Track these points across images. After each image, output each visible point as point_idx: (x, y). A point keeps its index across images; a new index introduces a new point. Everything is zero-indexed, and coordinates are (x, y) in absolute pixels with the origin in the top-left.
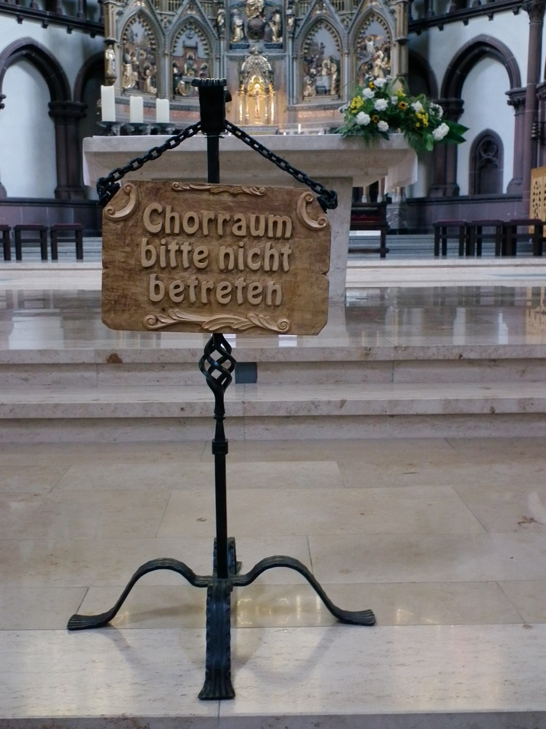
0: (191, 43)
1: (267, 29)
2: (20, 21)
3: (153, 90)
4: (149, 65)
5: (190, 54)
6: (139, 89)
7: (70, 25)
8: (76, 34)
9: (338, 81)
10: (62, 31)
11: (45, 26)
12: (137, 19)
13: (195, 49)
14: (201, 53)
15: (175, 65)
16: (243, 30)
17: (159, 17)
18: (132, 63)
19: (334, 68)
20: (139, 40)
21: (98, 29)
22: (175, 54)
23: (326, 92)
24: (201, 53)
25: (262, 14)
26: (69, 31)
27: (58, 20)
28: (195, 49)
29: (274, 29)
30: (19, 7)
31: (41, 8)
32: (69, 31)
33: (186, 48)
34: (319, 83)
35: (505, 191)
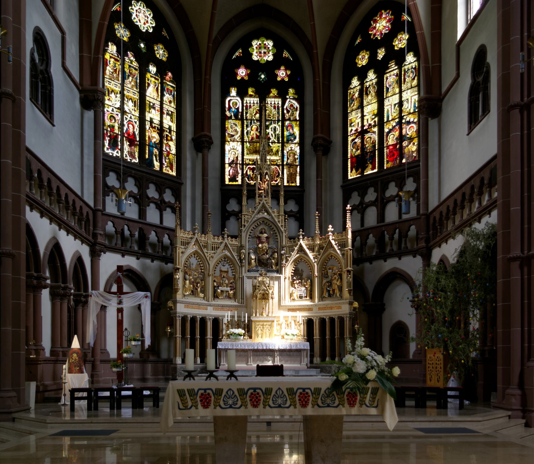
2: (123, 256)
3: (202, 295)
4: (200, 281)
6: (193, 294)
7: (153, 258)
8: (156, 263)
10: (148, 261)
11: (138, 259)
12: (193, 256)
13: (227, 272)
15: (214, 281)
16: (255, 261)
17: (206, 254)
18: (190, 280)
20: (194, 267)
21: (171, 259)
22: (215, 275)
24: (230, 274)
26: (152, 261)
27: (146, 255)
30: (123, 248)
31: (136, 248)
32: (152, 261)
33: (221, 271)
35: (411, 357)
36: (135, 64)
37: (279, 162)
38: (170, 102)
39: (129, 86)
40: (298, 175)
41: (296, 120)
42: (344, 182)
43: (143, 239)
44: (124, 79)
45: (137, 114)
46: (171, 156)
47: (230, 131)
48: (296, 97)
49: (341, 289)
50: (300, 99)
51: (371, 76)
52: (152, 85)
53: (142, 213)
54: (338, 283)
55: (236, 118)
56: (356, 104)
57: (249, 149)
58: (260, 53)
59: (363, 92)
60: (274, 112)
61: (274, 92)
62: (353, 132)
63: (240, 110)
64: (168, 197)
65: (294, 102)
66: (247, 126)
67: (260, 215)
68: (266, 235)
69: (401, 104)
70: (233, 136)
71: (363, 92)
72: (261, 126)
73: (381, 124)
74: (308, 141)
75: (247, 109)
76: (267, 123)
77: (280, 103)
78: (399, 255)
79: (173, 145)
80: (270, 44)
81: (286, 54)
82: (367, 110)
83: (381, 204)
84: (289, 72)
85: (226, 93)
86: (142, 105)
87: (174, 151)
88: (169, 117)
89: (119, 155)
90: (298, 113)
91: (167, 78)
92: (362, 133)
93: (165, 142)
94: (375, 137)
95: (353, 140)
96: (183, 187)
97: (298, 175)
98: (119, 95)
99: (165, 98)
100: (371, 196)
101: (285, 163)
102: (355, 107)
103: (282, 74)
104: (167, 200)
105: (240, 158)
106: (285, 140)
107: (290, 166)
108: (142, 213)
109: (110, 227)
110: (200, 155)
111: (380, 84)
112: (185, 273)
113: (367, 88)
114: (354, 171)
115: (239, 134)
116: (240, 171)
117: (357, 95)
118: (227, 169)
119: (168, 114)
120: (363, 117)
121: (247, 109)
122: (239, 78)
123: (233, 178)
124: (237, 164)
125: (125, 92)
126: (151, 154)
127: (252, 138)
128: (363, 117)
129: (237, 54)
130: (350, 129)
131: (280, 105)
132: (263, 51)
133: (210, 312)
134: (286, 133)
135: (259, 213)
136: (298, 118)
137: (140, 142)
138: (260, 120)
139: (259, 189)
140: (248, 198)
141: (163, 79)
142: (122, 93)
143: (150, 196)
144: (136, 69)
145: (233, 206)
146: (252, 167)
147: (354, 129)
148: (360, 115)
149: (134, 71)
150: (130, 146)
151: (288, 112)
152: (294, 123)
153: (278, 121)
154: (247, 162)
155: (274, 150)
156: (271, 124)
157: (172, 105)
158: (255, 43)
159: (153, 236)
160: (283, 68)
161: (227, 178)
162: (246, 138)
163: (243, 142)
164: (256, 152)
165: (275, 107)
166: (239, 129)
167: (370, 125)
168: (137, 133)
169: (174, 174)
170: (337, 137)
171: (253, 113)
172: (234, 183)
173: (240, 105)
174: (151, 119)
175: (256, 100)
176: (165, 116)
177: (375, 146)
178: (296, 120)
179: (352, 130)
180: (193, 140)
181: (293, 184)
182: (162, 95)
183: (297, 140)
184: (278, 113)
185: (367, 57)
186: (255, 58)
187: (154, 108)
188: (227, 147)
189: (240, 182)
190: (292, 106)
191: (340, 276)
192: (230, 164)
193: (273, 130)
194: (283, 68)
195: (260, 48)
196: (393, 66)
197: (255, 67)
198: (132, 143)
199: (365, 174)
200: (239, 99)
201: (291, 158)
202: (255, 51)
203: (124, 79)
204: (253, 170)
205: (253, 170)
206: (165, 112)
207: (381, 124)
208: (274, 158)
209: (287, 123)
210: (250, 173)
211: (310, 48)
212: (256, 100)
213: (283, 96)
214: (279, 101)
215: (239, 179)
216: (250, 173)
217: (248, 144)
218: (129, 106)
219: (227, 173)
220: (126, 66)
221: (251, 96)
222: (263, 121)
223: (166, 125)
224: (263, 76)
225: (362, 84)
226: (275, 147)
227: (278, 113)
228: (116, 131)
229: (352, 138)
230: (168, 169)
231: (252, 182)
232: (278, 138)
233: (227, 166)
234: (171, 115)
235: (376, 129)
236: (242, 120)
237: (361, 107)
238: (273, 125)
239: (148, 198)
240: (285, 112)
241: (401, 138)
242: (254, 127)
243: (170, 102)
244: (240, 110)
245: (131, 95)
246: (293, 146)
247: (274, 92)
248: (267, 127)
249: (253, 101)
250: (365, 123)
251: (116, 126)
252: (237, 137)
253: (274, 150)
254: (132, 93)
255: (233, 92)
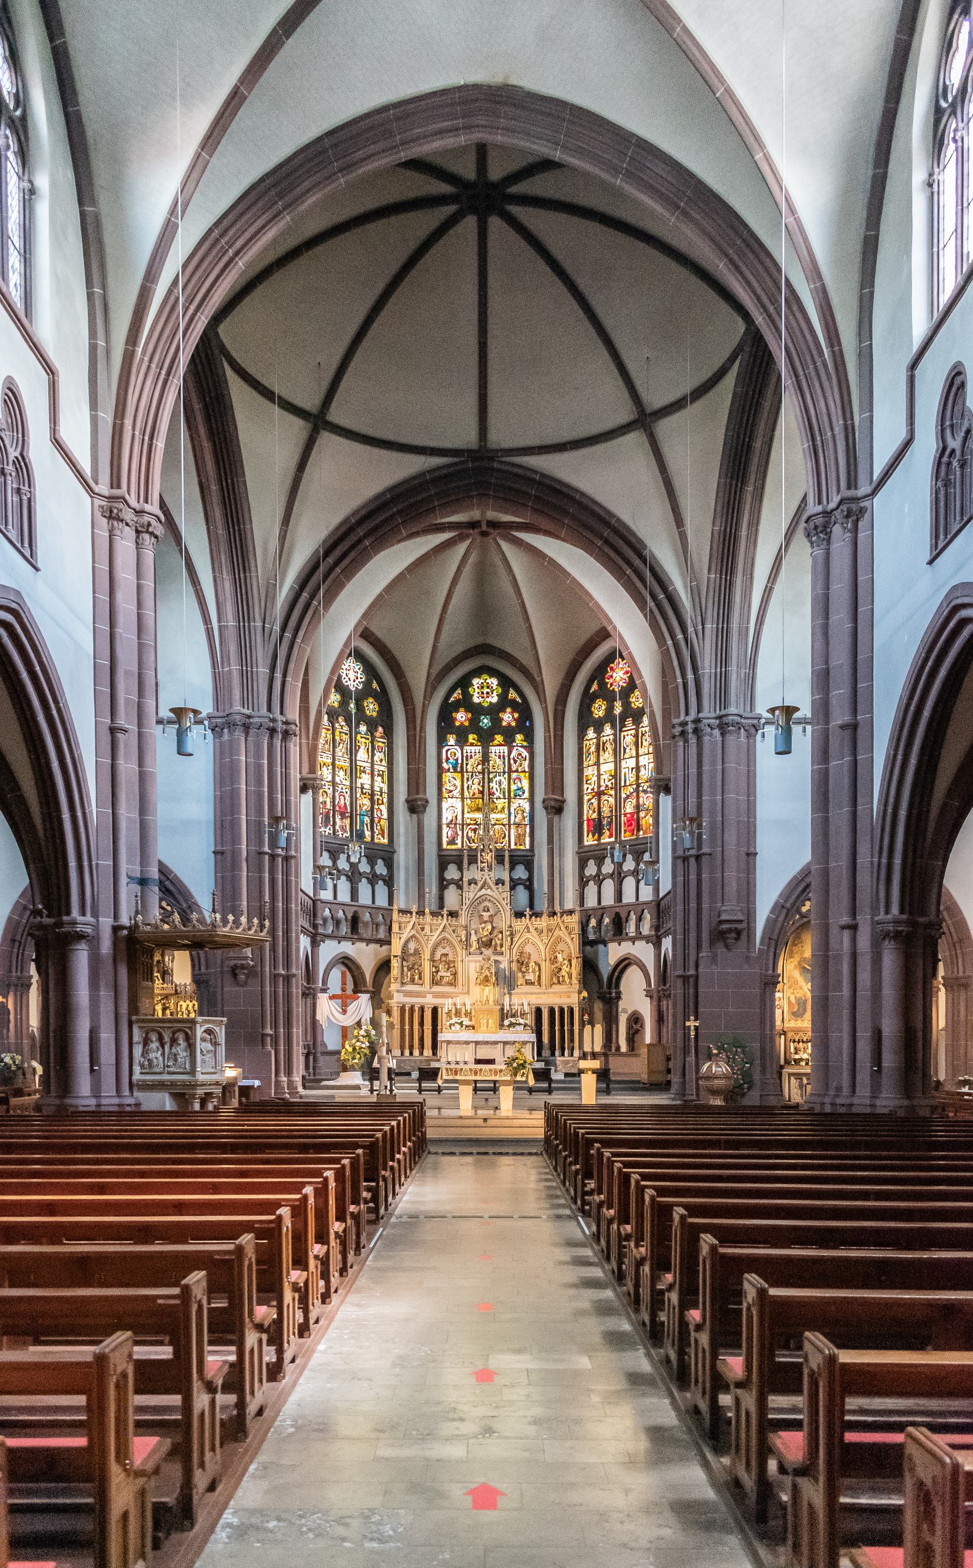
0: (445, 951)
1: (493, 943)
5: (444, 959)
7: (369, 941)
9: (539, 977)
14: (450, 958)
19: (537, 969)
23: (532, 984)
25: (490, 933)
28: (446, 955)
29: (499, 942)
34: (527, 978)
36: (346, 728)
37: (505, 821)
38: (381, 761)
39: (340, 754)
40: (527, 835)
41: (524, 772)
42: (579, 848)
43: (355, 922)
44: (334, 747)
45: (348, 783)
46: (382, 822)
47: (447, 786)
48: (525, 744)
49: (570, 977)
50: (530, 748)
51: (608, 730)
52: (362, 747)
53: (354, 894)
54: (568, 970)
55: (455, 771)
56: (593, 759)
57: (470, 807)
58: (483, 693)
59: (600, 747)
60: (499, 762)
61: (499, 738)
62: (589, 791)
63: (460, 761)
64: (381, 869)
65: (522, 750)
66: (468, 779)
67: (483, 892)
68: (489, 914)
69: (638, 768)
70: (451, 791)
71: (600, 747)
72: (483, 778)
73: (617, 787)
74: (540, 796)
75: (467, 759)
76: (491, 776)
77: (506, 751)
78: (633, 940)
79: (384, 808)
80: (494, 682)
81: (512, 694)
82: (604, 768)
83: (618, 876)
84: (516, 715)
85: (441, 741)
86: (353, 771)
87: (385, 816)
88: (380, 778)
89: (331, 832)
90: (527, 762)
91: (378, 734)
92: (599, 794)
93: (376, 807)
94: (612, 800)
95: (589, 800)
96: (395, 856)
97: (527, 835)
98: (330, 767)
99: (376, 758)
100: (608, 868)
101: (512, 822)
102: (591, 763)
103: (508, 718)
104: (378, 873)
105: (459, 817)
106: (512, 795)
107: (518, 825)
108: (354, 894)
109: (327, 912)
110: (415, 816)
111: (616, 741)
112: (403, 959)
113: (604, 744)
114: (590, 835)
115: (459, 788)
116: (460, 833)
117: (593, 749)
118: (445, 830)
119: (379, 775)
120: (599, 776)
121: (467, 759)
122: (457, 724)
123: (452, 842)
124: (456, 824)
125: (337, 762)
126: (362, 822)
127: (474, 794)
128: (599, 776)
129: (455, 695)
130: (586, 786)
131: (506, 754)
132: (485, 690)
133: (429, 1001)
134: (513, 787)
135: (481, 889)
136: (527, 770)
137: (351, 814)
138: (483, 773)
139: (482, 862)
140: (469, 864)
141: (372, 735)
142: (333, 764)
143: (362, 871)
144: (346, 734)
145: (452, 873)
146: (473, 827)
147: (591, 787)
148: (596, 772)
149: (344, 737)
150: (342, 819)
151: (515, 762)
152: (522, 775)
153: (504, 772)
154: (468, 821)
155: (500, 807)
156: (495, 776)
157: (384, 763)
158: (476, 682)
159: (367, 917)
160: (509, 710)
161: (445, 840)
162: (466, 794)
163: (463, 799)
164: (478, 809)
165: (499, 757)
166: (458, 783)
167: (607, 786)
168: (348, 804)
169: (386, 841)
170: (570, 794)
171: (473, 764)
172: (454, 847)
173: (459, 755)
174: (362, 784)
175: (478, 749)
176: (376, 778)
177: (612, 811)
178: (524, 772)
179: (588, 788)
180: (407, 801)
181: (522, 847)
182: (373, 755)
183: (526, 795)
184: (504, 763)
185: (604, 707)
186: (476, 700)
187: (364, 772)
188: (445, 805)
189: (459, 846)
190: (520, 754)
191: (570, 961)
192: (448, 825)
193: (498, 784)
194: (509, 710)
195: (482, 687)
196: (629, 722)
197: (476, 711)
198: (343, 816)
199: (602, 841)
200: (457, 747)
201: (519, 816)
202: (477, 690)
203: (334, 747)
204: (475, 830)
205: (475, 830)
206: (376, 773)
207: (617, 787)
208: (499, 816)
209: (514, 775)
210: (471, 834)
211: (538, 688)
212: (478, 749)
213: (509, 741)
214: (505, 749)
215: (459, 841)
216: (471, 834)
217: (469, 801)
218: (341, 776)
219: (444, 835)
220: (337, 733)
221: (472, 745)
222: (486, 773)
223: (377, 789)
224: (486, 721)
225: (598, 738)
226: (500, 803)
227: (504, 763)
228: (328, 807)
229: (590, 797)
230: (380, 836)
231: (474, 846)
232: (504, 793)
233: (444, 826)
234: (382, 776)
235: (613, 792)
236: (462, 772)
237: (598, 763)
238: (498, 778)
239: (360, 874)
240: (512, 762)
241: (638, 807)
242: (476, 781)
243: (381, 761)
244: (460, 761)
245: (342, 763)
246: (521, 802)
247: (499, 738)
248: (490, 780)
249: (475, 750)
250: (602, 783)
251: (328, 801)
252: (456, 793)
253: (500, 807)
254: (343, 762)
255: (452, 740)
